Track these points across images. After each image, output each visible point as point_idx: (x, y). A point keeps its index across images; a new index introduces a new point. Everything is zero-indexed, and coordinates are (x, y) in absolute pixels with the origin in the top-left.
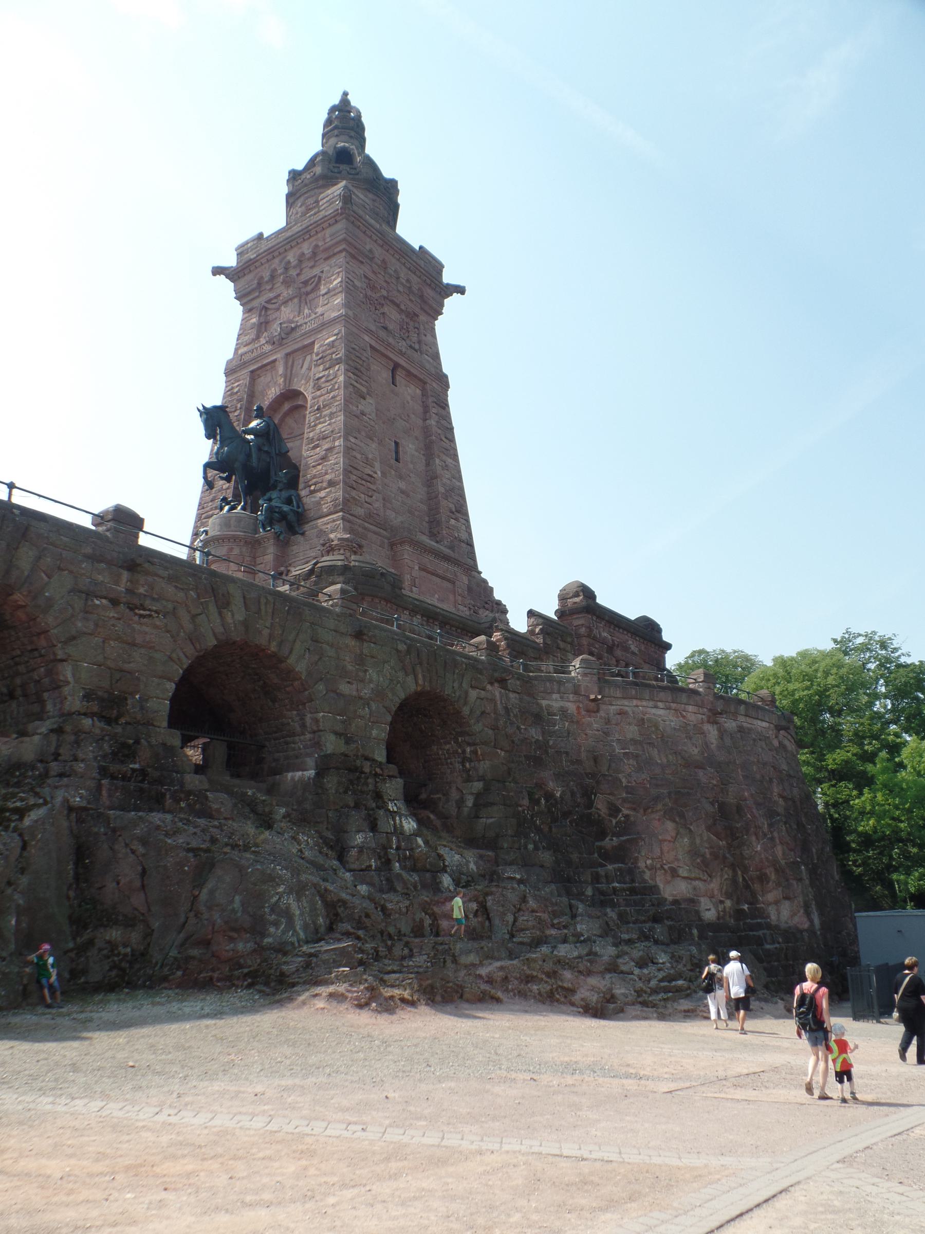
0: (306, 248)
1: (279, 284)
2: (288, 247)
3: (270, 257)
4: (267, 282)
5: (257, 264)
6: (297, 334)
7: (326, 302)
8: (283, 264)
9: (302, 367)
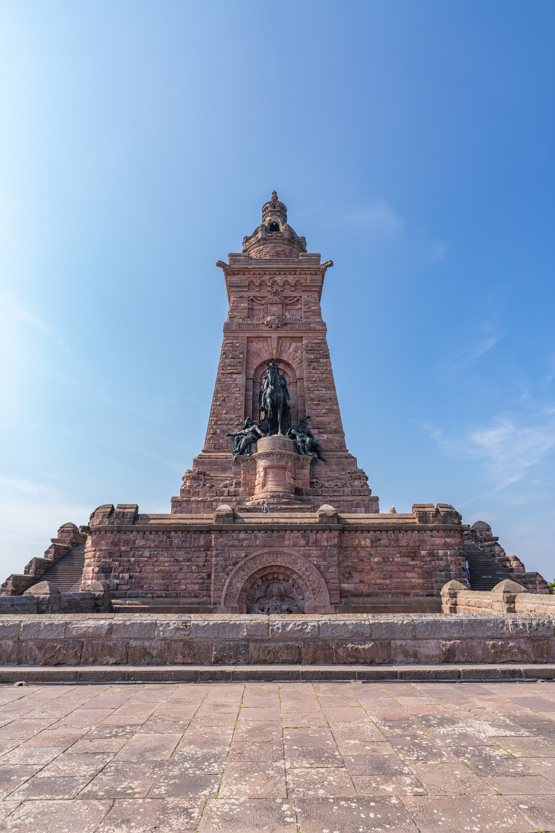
0: (291, 279)
1: (264, 291)
2: (277, 273)
3: (263, 273)
4: (257, 286)
5: (251, 273)
6: (288, 327)
7: (308, 317)
8: (271, 281)
9: (289, 348)
